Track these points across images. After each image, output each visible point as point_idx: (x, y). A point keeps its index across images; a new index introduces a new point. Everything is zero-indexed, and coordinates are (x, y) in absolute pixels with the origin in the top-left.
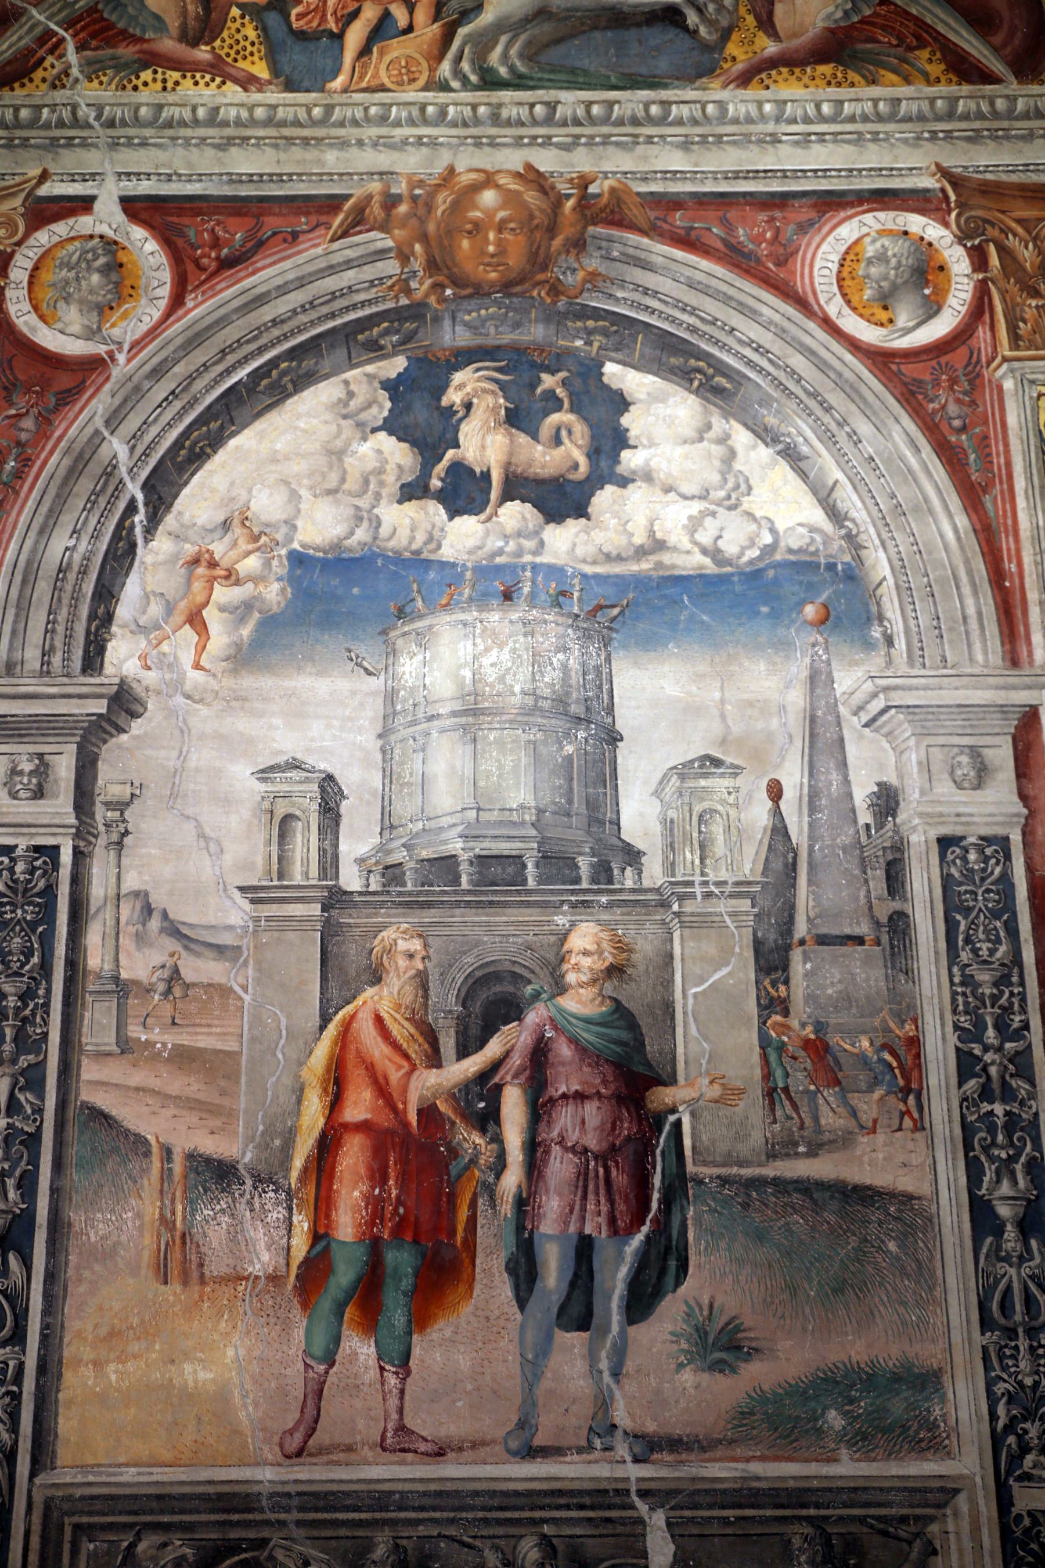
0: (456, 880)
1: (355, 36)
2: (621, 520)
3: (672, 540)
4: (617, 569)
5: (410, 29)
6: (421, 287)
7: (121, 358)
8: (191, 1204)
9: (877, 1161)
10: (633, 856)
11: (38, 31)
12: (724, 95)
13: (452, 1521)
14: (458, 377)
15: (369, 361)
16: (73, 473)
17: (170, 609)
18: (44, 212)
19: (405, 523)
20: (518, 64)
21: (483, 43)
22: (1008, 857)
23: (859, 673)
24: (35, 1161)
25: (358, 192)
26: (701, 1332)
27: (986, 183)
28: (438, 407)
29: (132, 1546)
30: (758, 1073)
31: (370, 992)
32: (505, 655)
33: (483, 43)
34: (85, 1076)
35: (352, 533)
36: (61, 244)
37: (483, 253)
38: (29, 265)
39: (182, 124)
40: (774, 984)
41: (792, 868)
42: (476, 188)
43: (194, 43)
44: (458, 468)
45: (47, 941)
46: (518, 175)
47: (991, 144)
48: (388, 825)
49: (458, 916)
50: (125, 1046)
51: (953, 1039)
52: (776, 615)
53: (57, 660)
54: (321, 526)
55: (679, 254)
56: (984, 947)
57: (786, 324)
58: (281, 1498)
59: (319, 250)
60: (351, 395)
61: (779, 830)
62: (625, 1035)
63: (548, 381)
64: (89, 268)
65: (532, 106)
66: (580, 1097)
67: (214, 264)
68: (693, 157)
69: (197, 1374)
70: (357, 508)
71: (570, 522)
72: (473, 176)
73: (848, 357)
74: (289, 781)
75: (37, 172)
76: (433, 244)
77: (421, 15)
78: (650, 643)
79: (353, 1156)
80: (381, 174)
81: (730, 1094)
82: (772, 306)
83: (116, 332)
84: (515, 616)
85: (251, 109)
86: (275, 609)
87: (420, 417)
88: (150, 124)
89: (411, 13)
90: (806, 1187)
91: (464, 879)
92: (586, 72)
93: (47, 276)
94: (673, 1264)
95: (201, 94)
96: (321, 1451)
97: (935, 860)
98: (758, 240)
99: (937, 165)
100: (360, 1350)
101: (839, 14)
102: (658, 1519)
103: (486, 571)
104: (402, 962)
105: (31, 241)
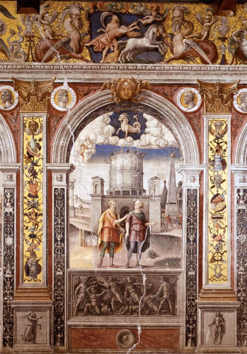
0: (120, 194)
1: (104, 52)
2: (145, 139)
3: (152, 143)
4: (144, 148)
6: (115, 99)
7: (69, 111)
8: (85, 237)
9: (175, 233)
10: (145, 191)
12: (164, 65)
13: (119, 275)
14: (121, 116)
15: (107, 112)
16: (63, 131)
17: (78, 153)
18: (56, 85)
19: (113, 140)
20: (131, 58)
21: (125, 54)
22: (197, 192)
23: (178, 165)
24: (64, 231)
25: (105, 82)
26: (151, 253)
27: (205, 83)
28: (118, 121)
29: (80, 277)
30: (160, 221)
31: (108, 209)
32: (127, 161)
34: (70, 220)
35: (105, 141)
37: (125, 94)
38: (54, 95)
39: (77, 69)
40: (163, 209)
41: (167, 193)
42: (124, 82)
44: (121, 131)
45: (64, 202)
46: (131, 79)
47: (206, 76)
48: (110, 186)
49: (120, 199)
50: (75, 216)
51: (187, 217)
52: (167, 156)
53: (62, 161)
54: (100, 140)
55: (156, 94)
57: (172, 107)
58: (98, 272)
59: (99, 93)
60: (105, 118)
61: (165, 188)
62: (143, 216)
63: (135, 116)
64: (63, 96)
65: (133, 66)
66: (136, 224)
67: (83, 95)
68: (159, 77)
69: (87, 258)
70: (106, 137)
71: (137, 140)
72: (124, 79)
73: (181, 113)
74: (96, 179)
75: (54, 78)
76: (117, 92)
77: (115, 49)
78: (148, 159)
80: (109, 79)
81: (156, 224)
82: (170, 104)
83: (68, 107)
84: (129, 155)
85: (88, 66)
86: (94, 153)
89: (114, 48)
90: (165, 236)
91: (121, 194)
92: (142, 60)
94: (148, 245)
96: (103, 267)
97: (187, 192)
99: (198, 79)
101: (184, 50)
102: (144, 275)
103: (124, 148)
104: (113, 205)
105: (54, 91)
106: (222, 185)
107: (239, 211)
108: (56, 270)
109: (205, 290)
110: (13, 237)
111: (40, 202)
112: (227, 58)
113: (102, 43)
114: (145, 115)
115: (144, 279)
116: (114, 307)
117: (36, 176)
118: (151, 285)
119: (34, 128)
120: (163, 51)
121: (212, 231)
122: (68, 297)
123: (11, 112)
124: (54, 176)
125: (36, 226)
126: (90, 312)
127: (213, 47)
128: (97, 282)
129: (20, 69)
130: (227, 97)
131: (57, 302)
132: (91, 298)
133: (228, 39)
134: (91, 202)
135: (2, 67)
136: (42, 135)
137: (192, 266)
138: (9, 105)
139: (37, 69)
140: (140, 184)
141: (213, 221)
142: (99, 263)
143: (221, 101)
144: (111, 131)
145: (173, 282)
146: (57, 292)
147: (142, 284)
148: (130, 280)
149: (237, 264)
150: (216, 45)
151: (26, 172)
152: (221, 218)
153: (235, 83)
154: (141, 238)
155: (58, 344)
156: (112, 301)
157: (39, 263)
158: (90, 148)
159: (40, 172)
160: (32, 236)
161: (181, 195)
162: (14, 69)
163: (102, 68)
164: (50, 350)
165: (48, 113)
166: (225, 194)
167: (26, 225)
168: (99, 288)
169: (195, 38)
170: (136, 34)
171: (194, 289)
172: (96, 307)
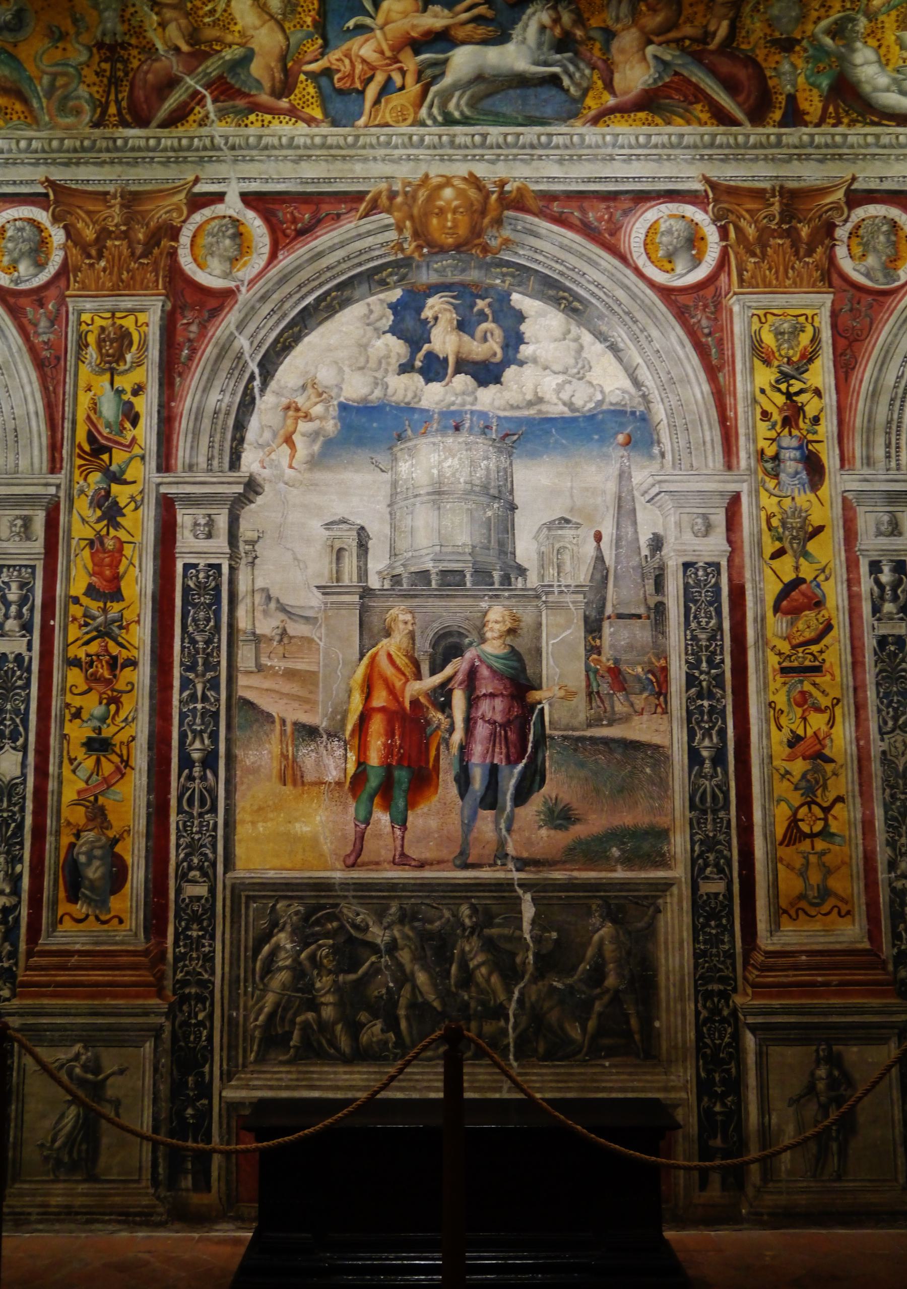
0: (429, 584)
1: (371, 92)
2: (519, 385)
5: (403, 88)
6: (410, 247)
7: (243, 289)
8: (296, 747)
9: (642, 729)
10: (522, 571)
11: (190, 91)
12: (583, 130)
14: (431, 301)
15: (381, 292)
16: (220, 357)
17: (275, 435)
18: (198, 202)
21: (445, 96)
22: (719, 574)
23: (646, 472)
24: (217, 724)
27: (730, 187)
30: (584, 684)
31: (385, 641)
32: (456, 461)
33: (445, 96)
36: (207, 222)
37: (444, 227)
38: (190, 234)
39: (274, 147)
41: (606, 578)
42: (440, 187)
43: (279, 97)
44: (430, 355)
45: (218, 613)
46: (465, 179)
47: (734, 163)
48: (393, 554)
49: (431, 602)
50: (260, 668)
51: (685, 668)
52: (602, 441)
53: (215, 463)
54: (356, 388)
55: (555, 228)
56: (704, 621)
59: (352, 225)
60: (371, 312)
61: (600, 558)
62: (515, 664)
63: (481, 304)
66: (492, 696)
69: (302, 828)
71: (491, 386)
72: (440, 179)
73: (648, 291)
74: (340, 530)
75: (191, 178)
77: (410, 79)
78: (533, 455)
79: (377, 725)
81: (570, 695)
82: (607, 260)
83: (240, 274)
84: (461, 440)
85: (312, 138)
87: (409, 325)
88: (255, 148)
90: (607, 742)
92: (504, 115)
93: (202, 241)
94: (538, 778)
95: (284, 129)
96: (364, 864)
98: (600, 220)
100: (381, 818)
102: (528, 897)
103: (446, 414)
104: (401, 626)
105: (191, 220)
106: (811, 546)
107: (882, 641)
108: (183, 877)
109: (769, 954)
110: (24, 748)
111: (128, 615)
112: (804, 105)
113: (364, 61)
114: (517, 299)
115: (528, 911)
116: (410, 1026)
117: (119, 519)
118: (554, 935)
119: (116, 347)
120: (577, 85)
121: (783, 721)
122: (226, 988)
123: (38, 295)
124: (184, 517)
125: (113, 707)
126: (315, 1049)
127: (750, 70)
128: (342, 927)
129: (75, 150)
130: (811, 235)
131: (185, 1008)
132: (319, 990)
133: (805, 43)
134: (321, 615)
135: (14, 146)
136: (149, 374)
137: (711, 857)
138: (32, 270)
139: (133, 149)
140: (505, 549)
141: (785, 683)
142: (349, 849)
143: (792, 246)
144: (393, 354)
145: (641, 925)
146: (185, 966)
147: (518, 933)
148: (470, 917)
149: (889, 851)
150: (764, 65)
151: (82, 505)
152: (817, 669)
153: (836, 187)
154: (512, 750)
155: (187, 1182)
156: (403, 1002)
157: (118, 849)
158: (318, 418)
159: (132, 505)
160: (97, 746)
161: (659, 584)
162: (53, 151)
163: (362, 141)
164: (154, 1206)
165: (167, 296)
166: (827, 579)
167: (77, 702)
168: (352, 949)
169: (687, 42)
170: (481, 31)
171: (725, 952)
172: (339, 1027)
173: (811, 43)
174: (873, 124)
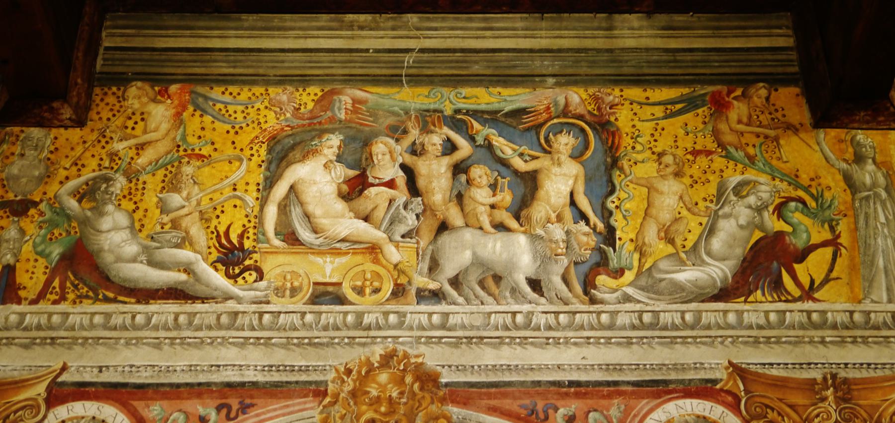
112: (22, 278)
133: (43, 206)
153: (39, 379)
173: (51, 206)
174: (107, 300)
